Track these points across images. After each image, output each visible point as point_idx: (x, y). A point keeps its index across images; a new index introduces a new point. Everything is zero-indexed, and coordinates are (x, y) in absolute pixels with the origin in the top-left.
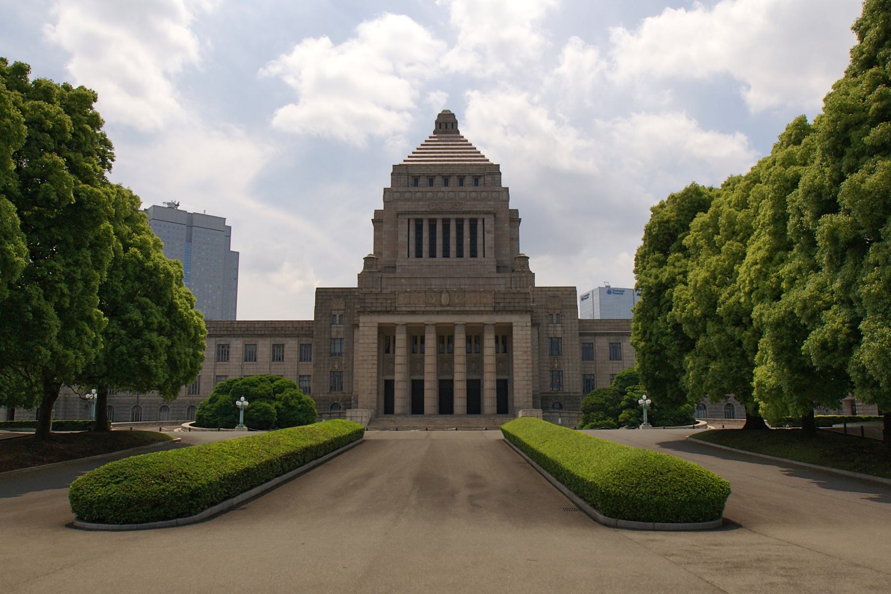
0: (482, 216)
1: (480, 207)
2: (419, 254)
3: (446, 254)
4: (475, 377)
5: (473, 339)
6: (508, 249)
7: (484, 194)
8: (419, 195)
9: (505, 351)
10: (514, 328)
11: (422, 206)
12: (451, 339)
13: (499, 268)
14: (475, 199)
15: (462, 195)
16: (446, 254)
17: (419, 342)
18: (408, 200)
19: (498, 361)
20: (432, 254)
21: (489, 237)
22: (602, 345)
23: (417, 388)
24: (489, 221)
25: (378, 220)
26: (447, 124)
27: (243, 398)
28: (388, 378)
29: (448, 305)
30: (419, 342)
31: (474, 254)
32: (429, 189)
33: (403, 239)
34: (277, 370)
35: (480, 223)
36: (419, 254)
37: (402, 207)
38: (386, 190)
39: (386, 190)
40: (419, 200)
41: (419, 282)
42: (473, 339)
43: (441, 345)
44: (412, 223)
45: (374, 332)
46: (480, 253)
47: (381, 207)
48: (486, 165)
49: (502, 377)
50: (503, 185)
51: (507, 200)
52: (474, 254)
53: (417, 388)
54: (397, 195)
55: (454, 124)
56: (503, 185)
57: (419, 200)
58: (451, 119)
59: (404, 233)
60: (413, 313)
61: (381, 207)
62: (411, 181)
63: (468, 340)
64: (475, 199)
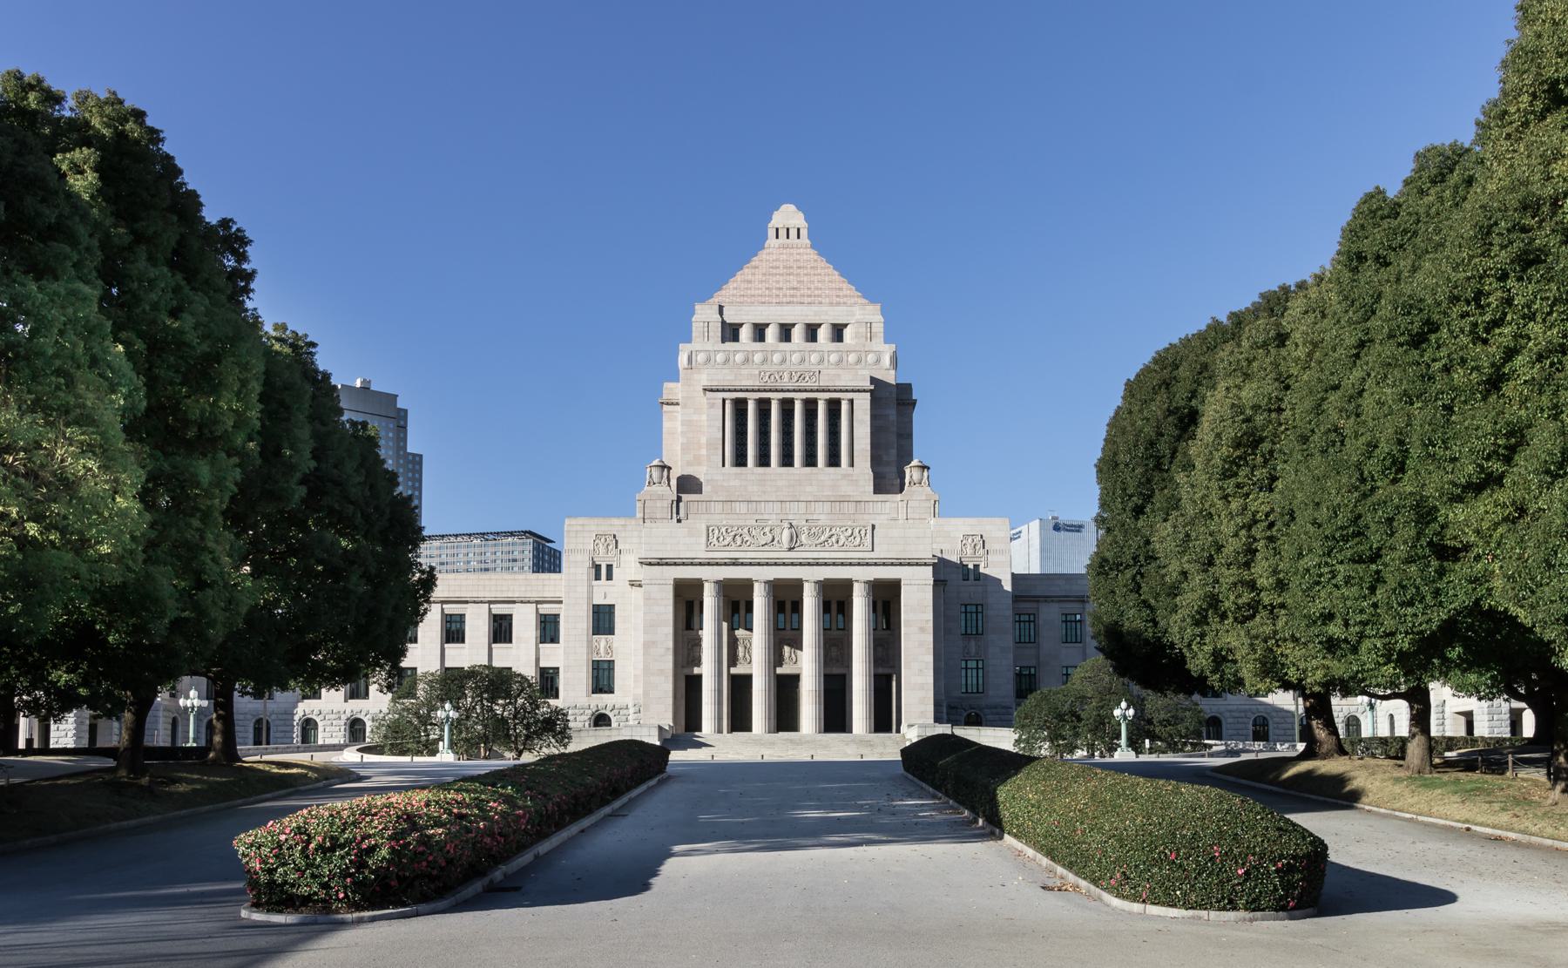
0: (850, 395)
1: (845, 380)
2: (740, 460)
4: (836, 671)
5: (834, 607)
6: (894, 452)
9: (888, 627)
12: (797, 607)
17: (742, 611)
22: (1050, 615)
27: (448, 706)
29: (791, 549)
30: (742, 611)
31: (834, 460)
34: (504, 657)
36: (740, 460)
41: (743, 507)
42: (834, 607)
43: (781, 617)
49: (881, 671)
52: (834, 460)
53: (740, 688)
60: (735, 563)
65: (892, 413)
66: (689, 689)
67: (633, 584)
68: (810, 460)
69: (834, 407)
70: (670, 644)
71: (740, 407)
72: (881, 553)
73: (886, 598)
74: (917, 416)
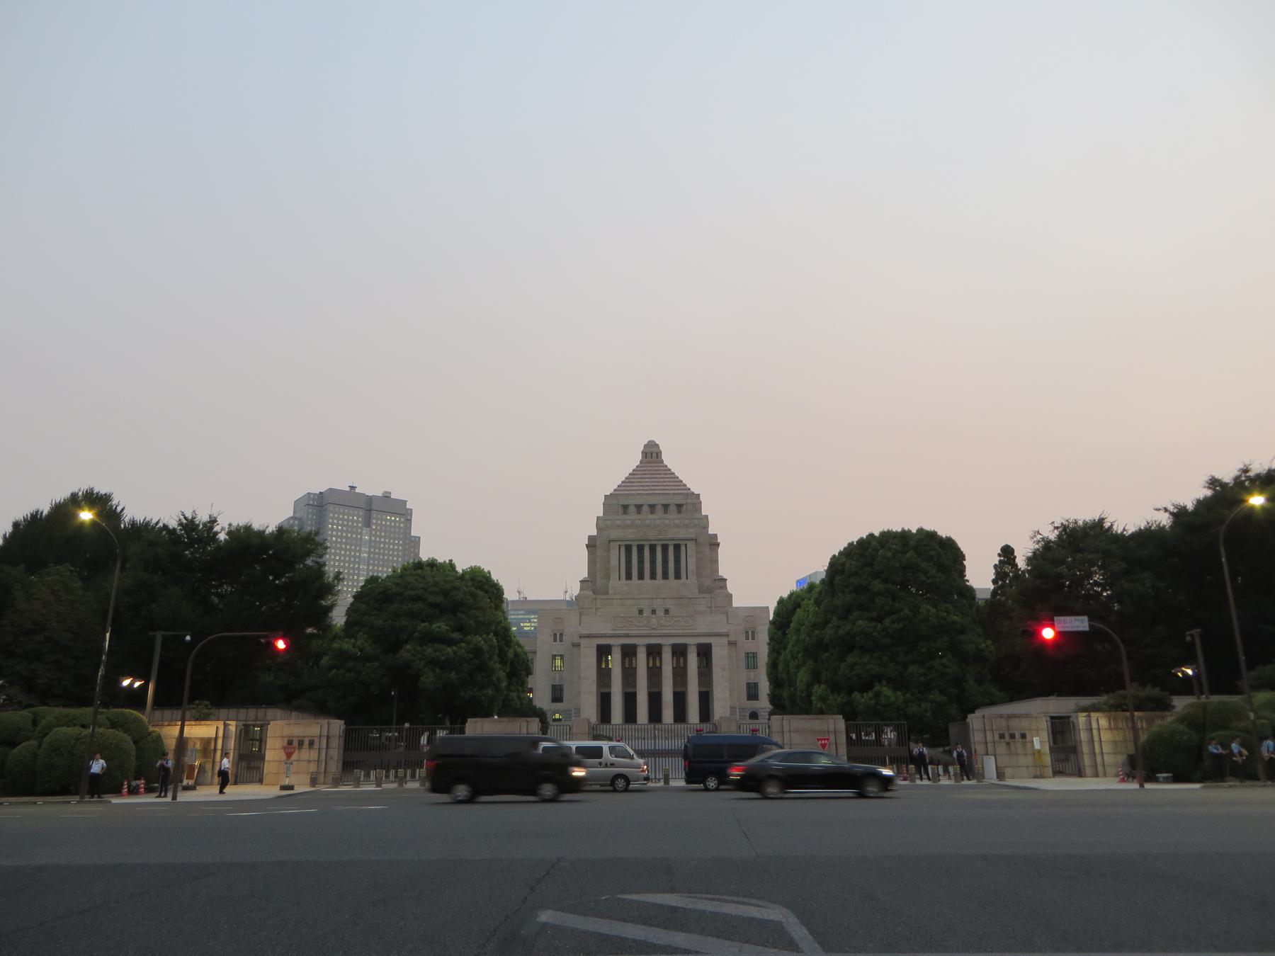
1: (682, 534)
2: (629, 577)
3: (653, 576)
4: (679, 689)
7: (686, 522)
8: (628, 522)
10: (714, 649)
11: (630, 534)
13: (701, 591)
14: (678, 526)
15: (667, 522)
16: (653, 576)
18: (619, 526)
19: (701, 674)
20: (641, 577)
21: (692, 562)
23: (630, 700)
24: (691, 546)
25: (592, 545)
26: (652, 454)
28: (606, 690)
31: (678, 576)
32: (637, 517)
33: (614, 562)
35: (683, 548)
36: (629, 577)
37: (615, 534)
38: (598, 518)
39: (598, 518)
40: (627, 527)
41: (629, 602)
44: (623, 550)
45: (594, 652)
46: (683, 575)
47: (594, 533)
48: (687, 495)
49: (703, 689)
50: (704, 513)
51: (706, 527)
52: (678, 576)
53: (630, 700)
54: (609, 523)
55: (659, 454)
56: (704, 513)
57: (627, 527)
58: (655, 450)
59: (616, 558)
60: (627, 636)
61: (594, 533)
62: (620, 509)
63: (674, 654)
64: (678, 526)
65: (707, 550)
66: (605, 701)
67: (577, 645)
68: (665, 576)
69: (677, 547)
70: (595, 678)
71: (628, 549)
72: (701, 629)
73: (705, 653)
74: (721, 551)
